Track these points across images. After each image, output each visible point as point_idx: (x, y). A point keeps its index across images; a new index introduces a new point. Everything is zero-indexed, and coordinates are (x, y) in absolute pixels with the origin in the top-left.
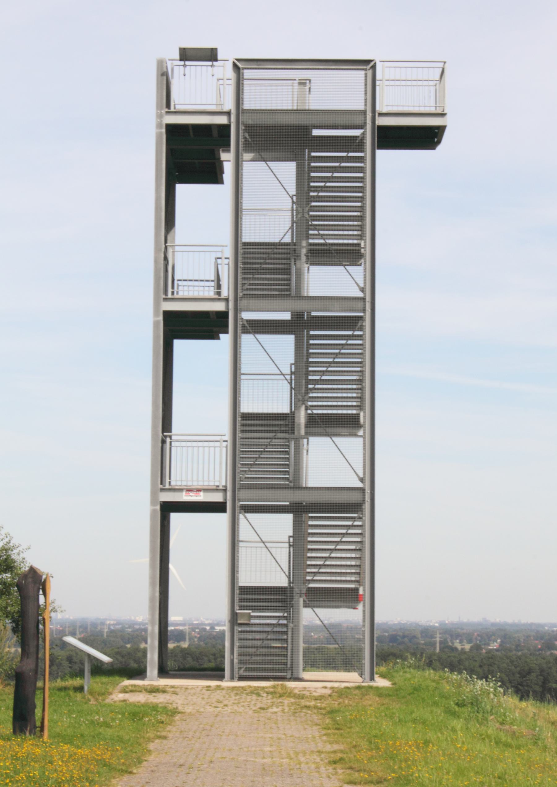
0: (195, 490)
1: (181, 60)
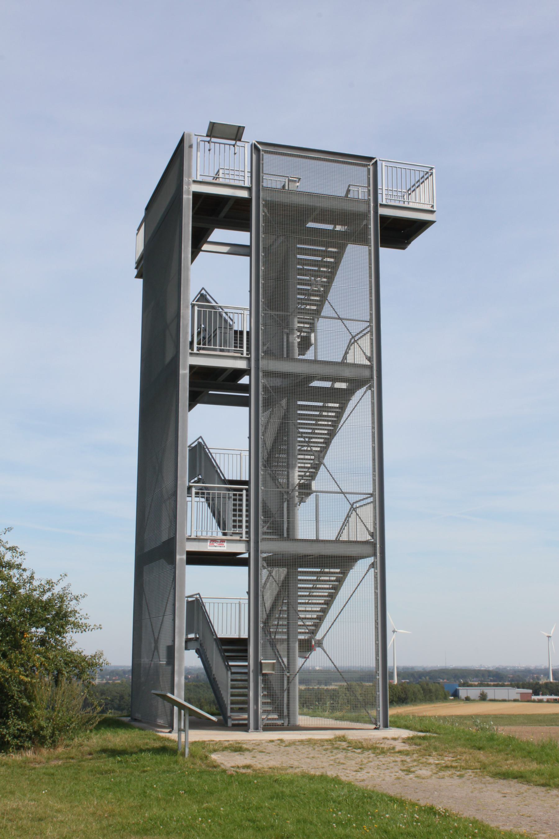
0: (219, 541)
1: (207, 136)
